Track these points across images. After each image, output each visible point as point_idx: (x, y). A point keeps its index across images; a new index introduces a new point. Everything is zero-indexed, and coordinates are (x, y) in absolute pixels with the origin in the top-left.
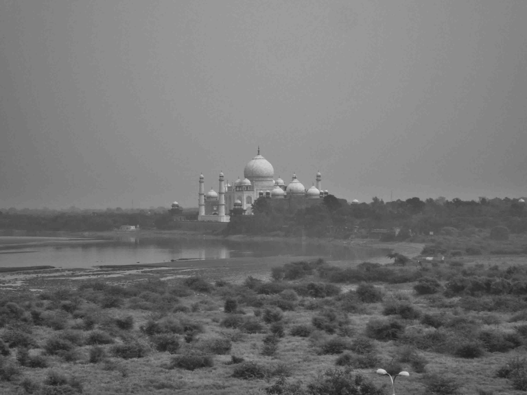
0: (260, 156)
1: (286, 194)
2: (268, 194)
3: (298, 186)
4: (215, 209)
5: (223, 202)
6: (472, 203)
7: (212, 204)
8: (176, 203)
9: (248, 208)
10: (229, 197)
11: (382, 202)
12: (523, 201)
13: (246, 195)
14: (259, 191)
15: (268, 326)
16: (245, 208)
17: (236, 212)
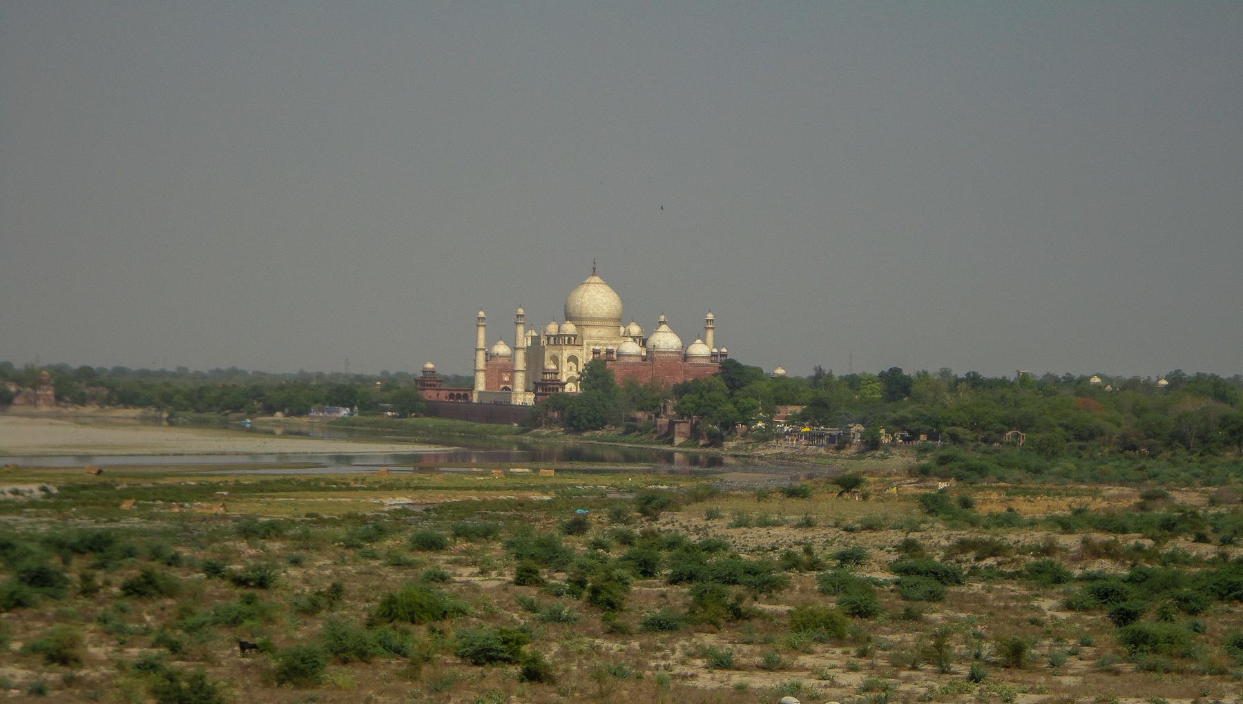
0: (597, 279)
1: (644, 354)
2: (609, 352)
3: (666, 340)
4: (506, 379)
5: (520, 364)
6: (1003, 383)
7: (500, 369)
8: (430, 366)
9: (570, 380)
10: (535, 354)
11: (830, 376)
12: (1097, 380)
13: (567, 352)
14: (592, 347)
15: (179, 636)
16: (564, 379)
17: (545, 386)
